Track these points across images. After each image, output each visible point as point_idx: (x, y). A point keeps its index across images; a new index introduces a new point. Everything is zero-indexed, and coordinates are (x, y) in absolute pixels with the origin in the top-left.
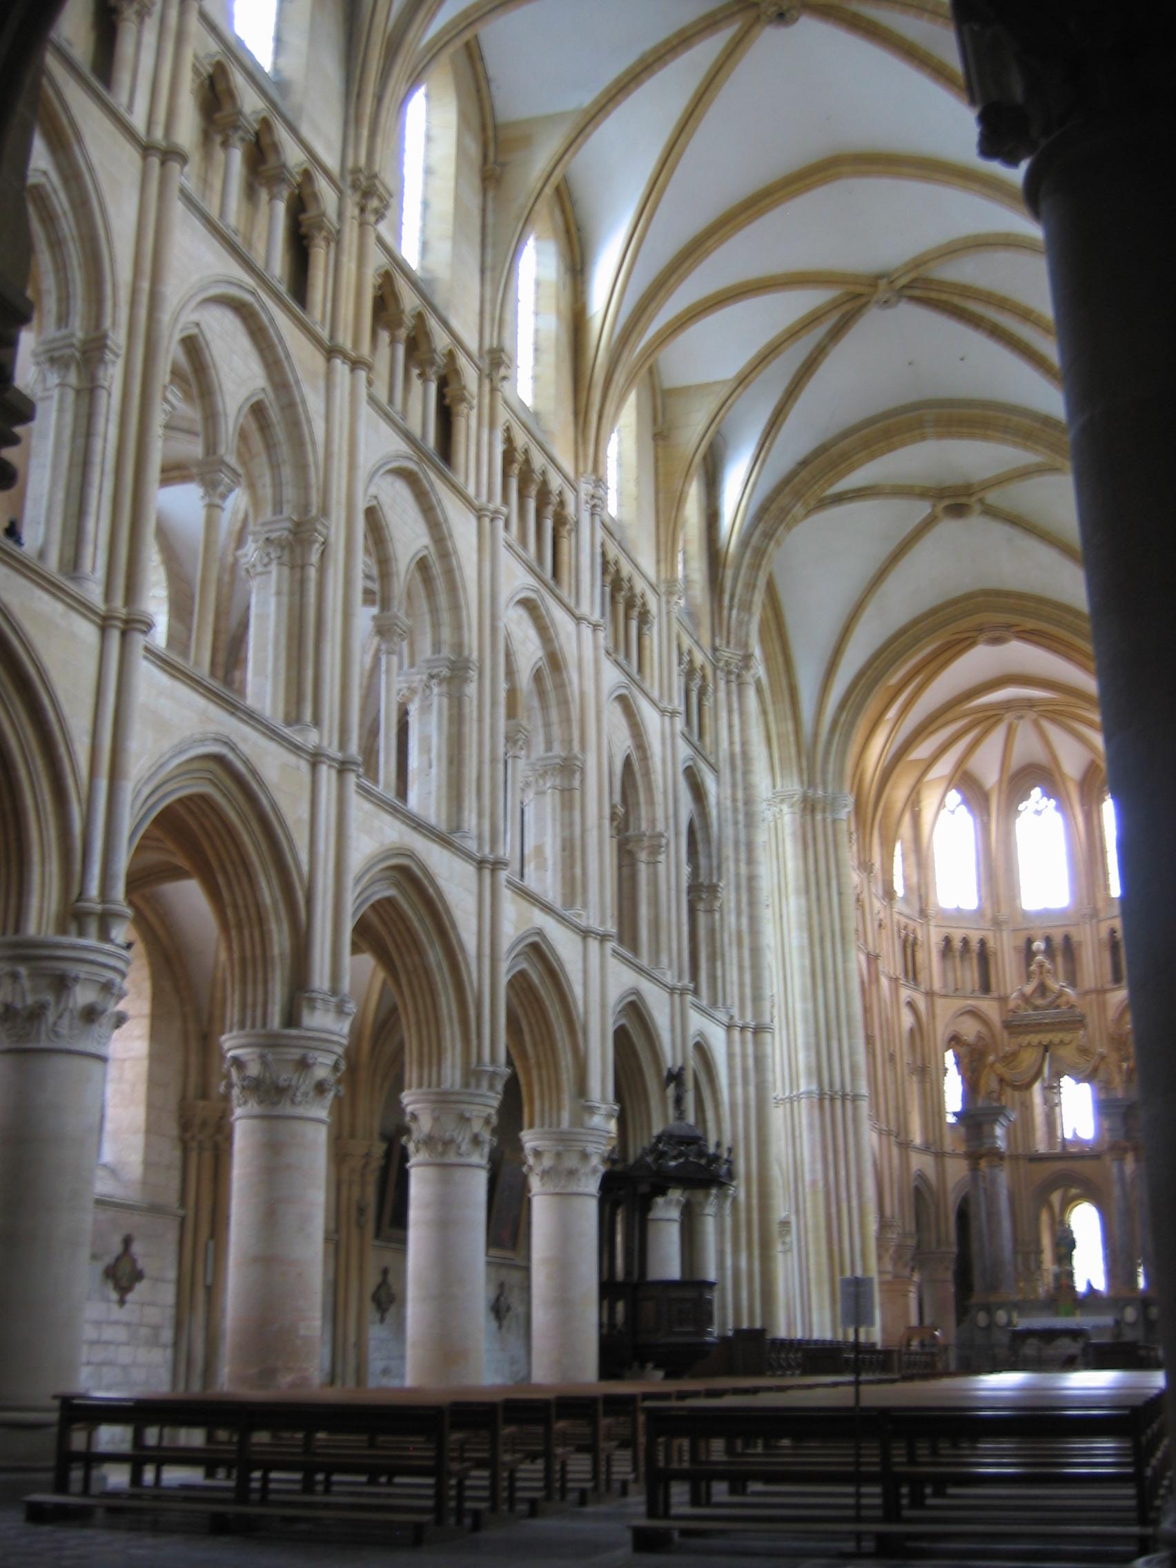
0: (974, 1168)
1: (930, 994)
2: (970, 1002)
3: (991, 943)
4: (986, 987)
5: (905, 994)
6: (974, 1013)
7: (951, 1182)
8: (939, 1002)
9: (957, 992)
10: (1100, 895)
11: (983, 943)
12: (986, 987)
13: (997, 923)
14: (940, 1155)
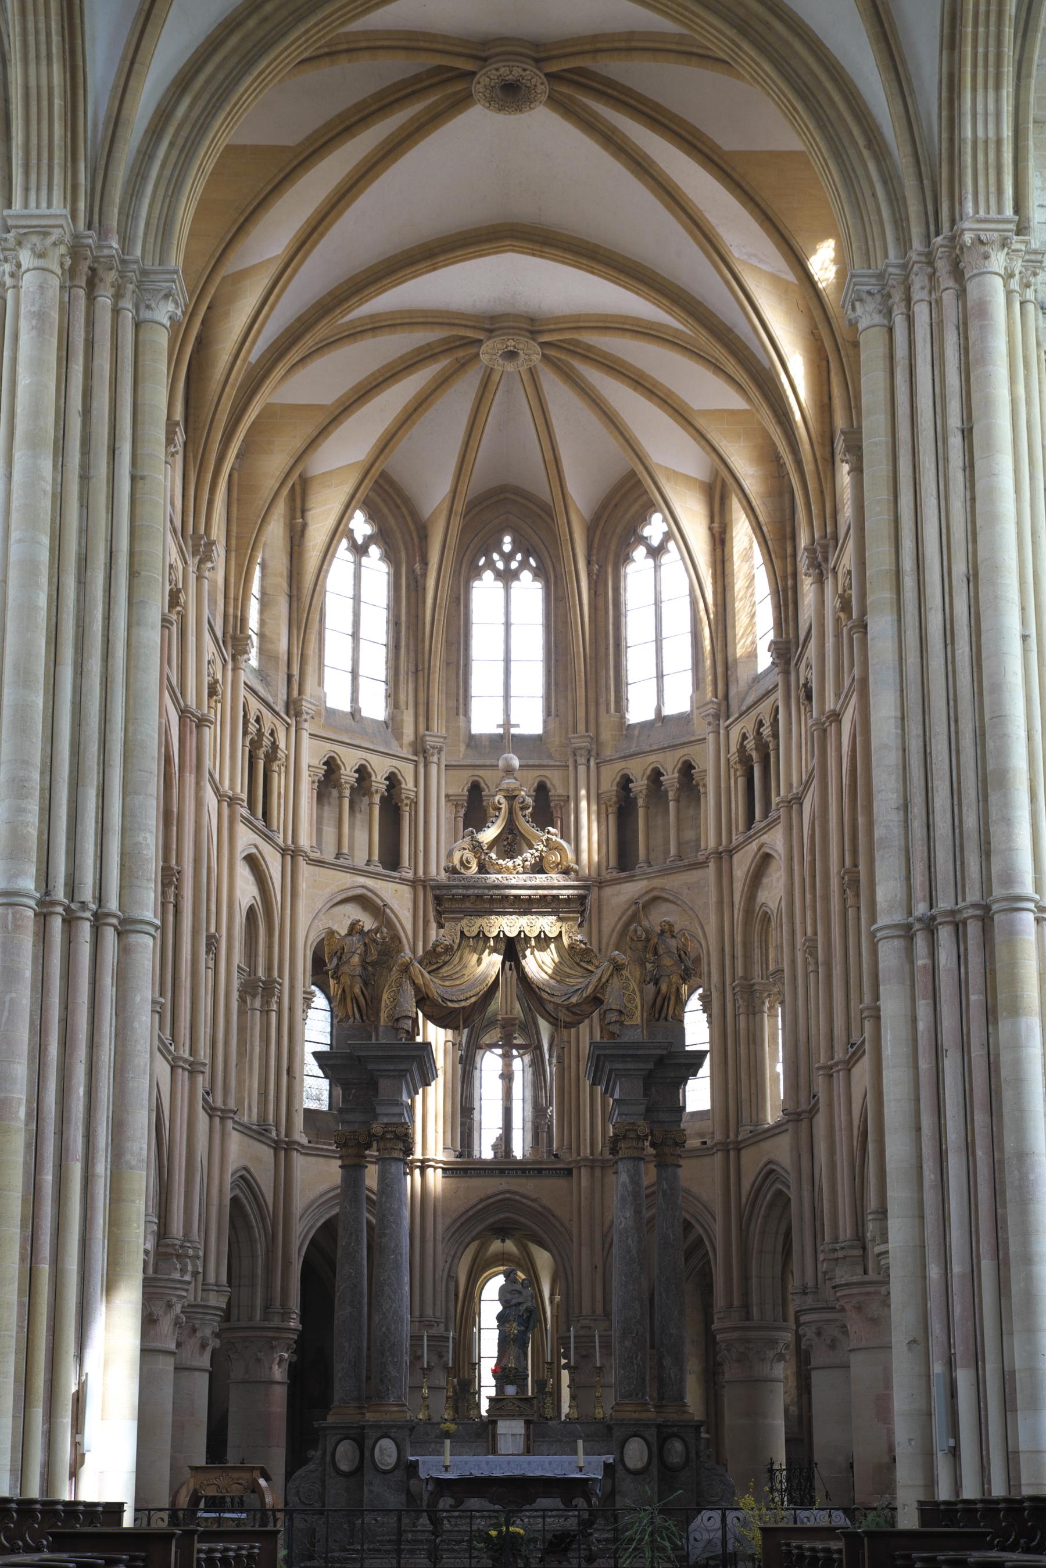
0: (353, 1171)
1: (291, 853)
2: (362, 880)
4: (391, 859)
5: (246, 838)
6: (363, 901)
7: (300, 1201)
8: (305, 870)
9: (340, 862)
10: (607, 721)
11: (393, 781)
12: (391, 859)
14: (284, 1148)
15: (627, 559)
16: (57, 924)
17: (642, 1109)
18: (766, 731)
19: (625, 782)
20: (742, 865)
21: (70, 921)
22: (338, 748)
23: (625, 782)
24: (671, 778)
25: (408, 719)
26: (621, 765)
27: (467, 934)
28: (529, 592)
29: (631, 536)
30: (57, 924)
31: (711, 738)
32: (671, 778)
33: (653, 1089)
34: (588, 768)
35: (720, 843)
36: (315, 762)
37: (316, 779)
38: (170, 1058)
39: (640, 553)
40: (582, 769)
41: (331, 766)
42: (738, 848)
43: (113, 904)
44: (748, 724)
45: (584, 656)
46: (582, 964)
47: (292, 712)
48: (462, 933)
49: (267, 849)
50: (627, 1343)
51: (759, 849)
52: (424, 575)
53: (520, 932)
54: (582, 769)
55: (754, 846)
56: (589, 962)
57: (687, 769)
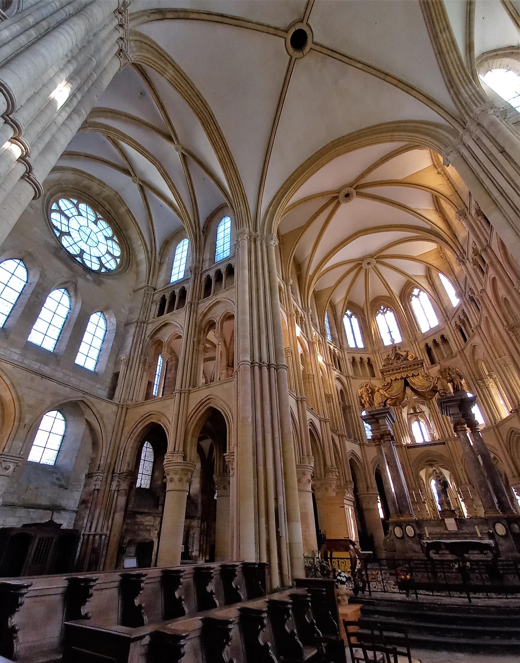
1: (347, 377)
3: (372, 358)
7: (369, 460)
11: (369, 359)
13: (374, 352)
15: (411, 300)
16: (257, 368)
17: (461, 415)
18: (462, 317)
19: (427, 345)
20: (467, 352)
21: (260, 367)
22: (354, 354)
23: (427, 345)
24: (439, 340)
25: (369, 345)
26: (424, 341)
28: (390, 316)
29: (410, 295)
30: (257, 368)
31: (447, 326)
32: (439, 340)
35: (458, 349)
39: (414, 298)
40: (414, 345)
41: (354, 359)
42: (464, 349)
43: (273, 361)
44: (456, 319)
45: (407, 323)
49: (342, 377)
51: (471, 345)
52: (365, 318)
54: (414, 345)
55: (469, 345)
57: (442, 337)
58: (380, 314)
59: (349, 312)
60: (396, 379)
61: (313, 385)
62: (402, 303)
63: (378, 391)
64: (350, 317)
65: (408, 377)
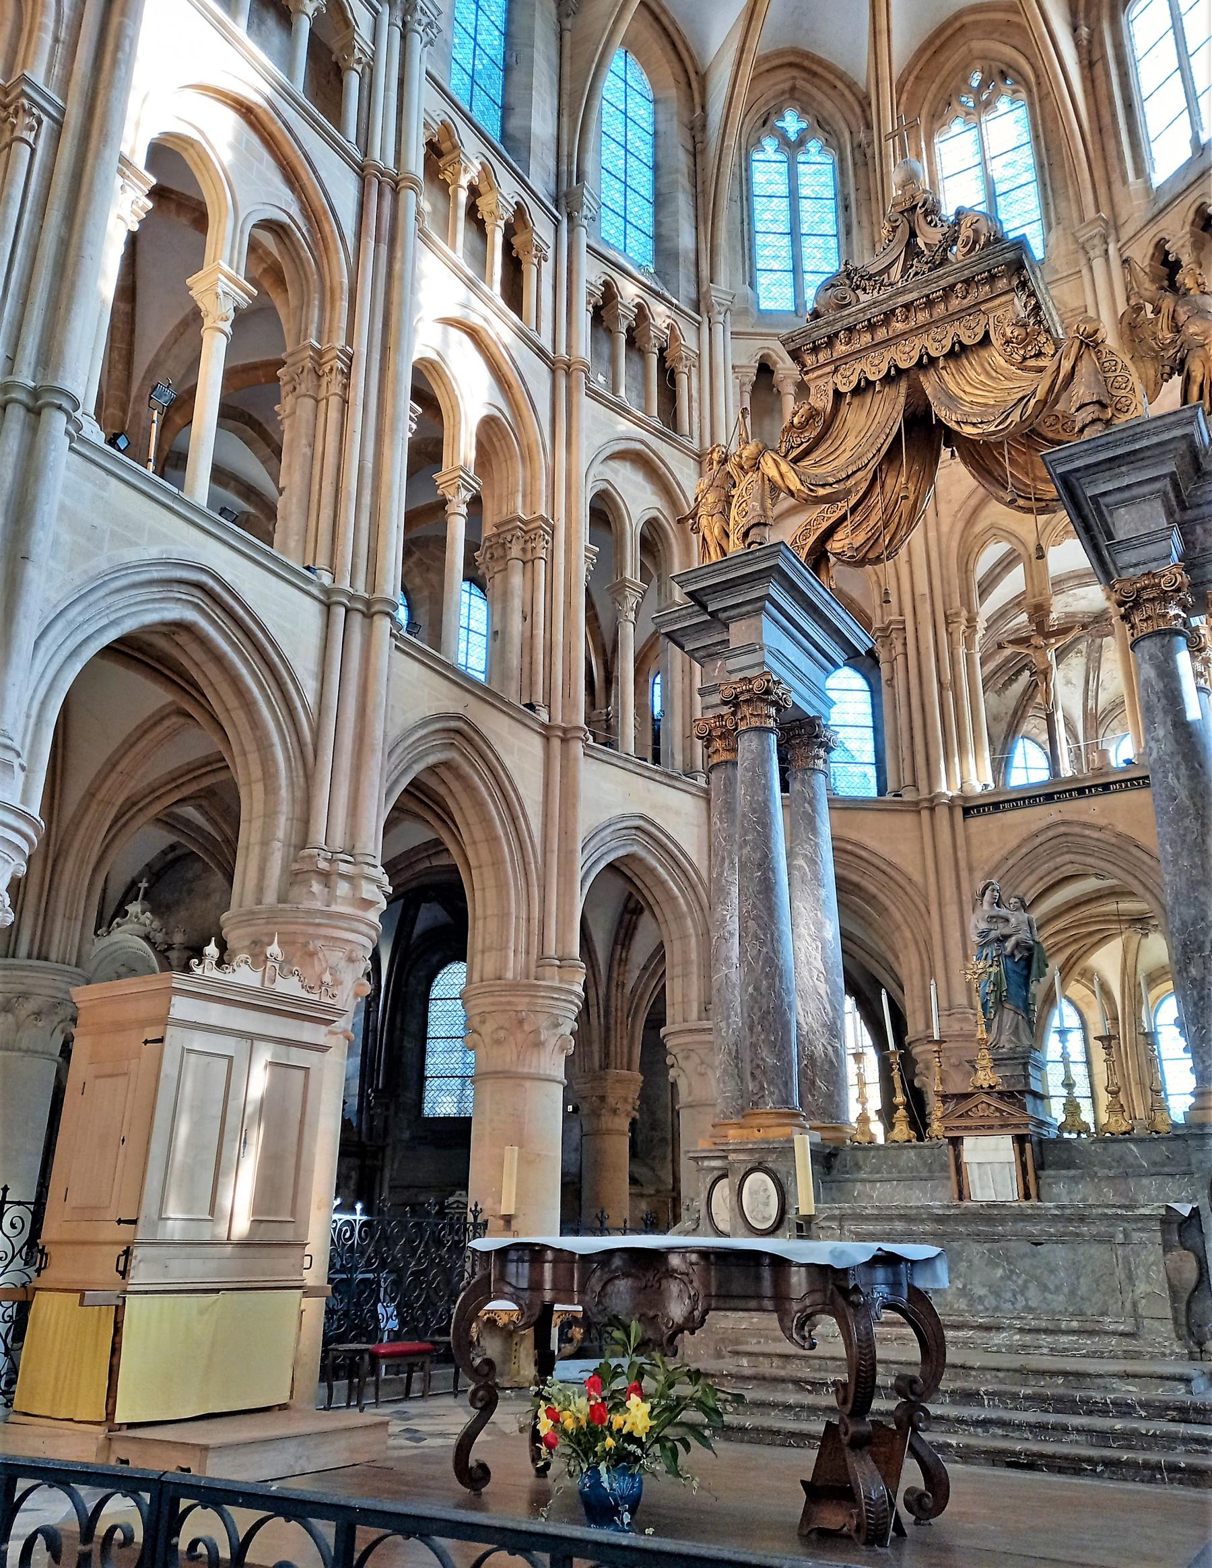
27: (842, 389)
33: (1199, 530)
34: (1107, 260)
36: (744, 361)
37: (747, 380)
38: (315, 591)
40: (1098, 264)
46: (1031, 363)
47: (702, 309)
48: (836, 391)
49: (665, 450)
50: (1193, 971)
53: (921, 357)
54: (1098, 264)
56: (1039, 354)
58: (957, 126)
59: (792, 123)
60: (863, 389)
61: (334, 415)
62: (1075, 29)
63: (756, 466)
64: (792, 147)
65: (926, 363)
